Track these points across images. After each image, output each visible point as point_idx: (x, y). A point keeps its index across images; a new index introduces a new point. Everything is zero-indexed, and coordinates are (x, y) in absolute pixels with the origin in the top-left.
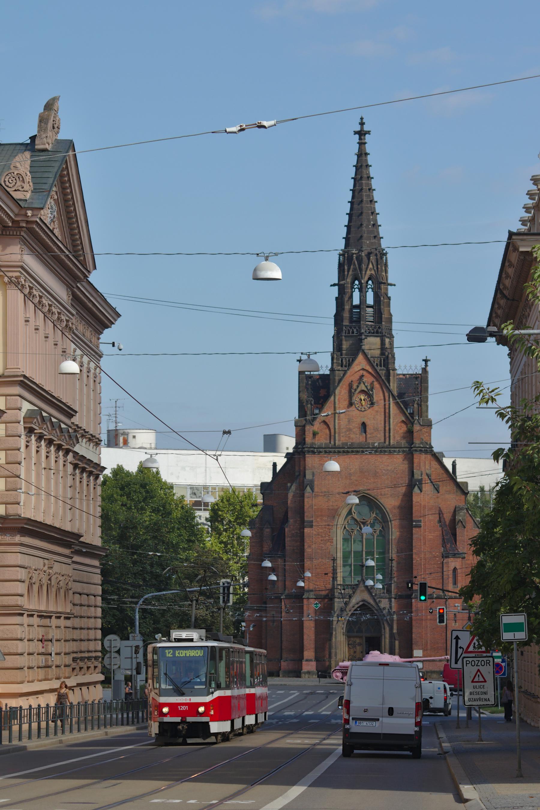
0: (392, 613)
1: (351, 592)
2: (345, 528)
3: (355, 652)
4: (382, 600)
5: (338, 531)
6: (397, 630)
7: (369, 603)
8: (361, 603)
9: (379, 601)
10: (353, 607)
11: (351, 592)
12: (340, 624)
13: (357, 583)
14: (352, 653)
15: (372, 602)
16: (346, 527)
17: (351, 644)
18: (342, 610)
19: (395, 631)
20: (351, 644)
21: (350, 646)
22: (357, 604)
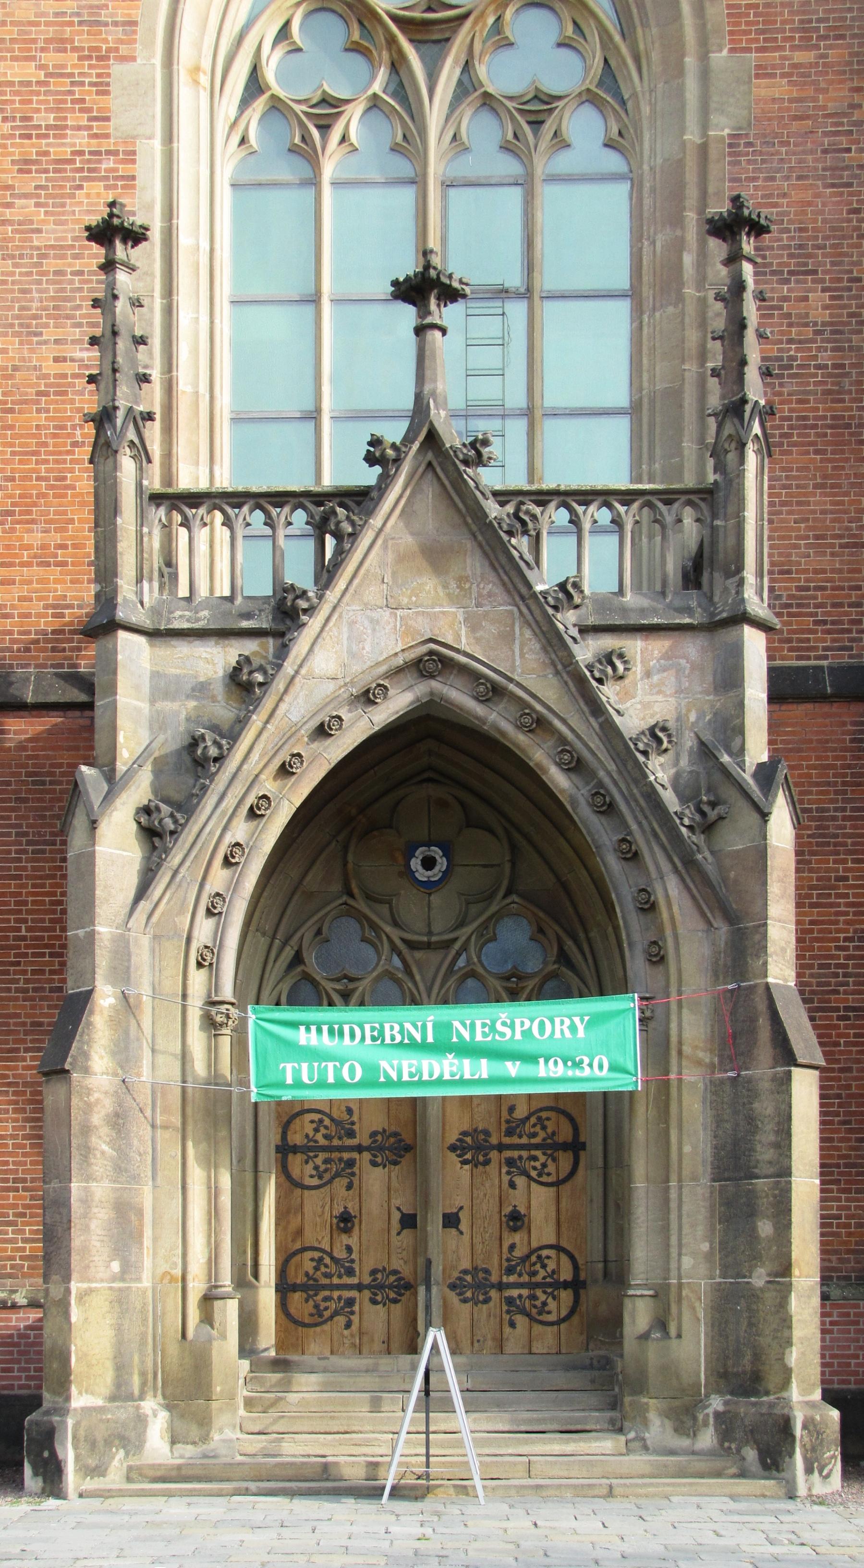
0: (747, 777)
1: (300, 572)
2: (255, 85)
3: (345, 1222)
4: (635, 647)
5: (190, 100)
6: (802, 969)
7: (493, 692)
8: (398, 703)
9: (608, 658)
10: (322, 732)
11: (300, 572)
12: (174, 898)
13: (369, 476)
14: (318, 1234)
15: (523, 666)
16: (270, 74)
17: (308, 1149)
18: (195, 762)
19: (780, 970)
20: (308, 1149)
21: (296, 1163)
22: (367, 698)
